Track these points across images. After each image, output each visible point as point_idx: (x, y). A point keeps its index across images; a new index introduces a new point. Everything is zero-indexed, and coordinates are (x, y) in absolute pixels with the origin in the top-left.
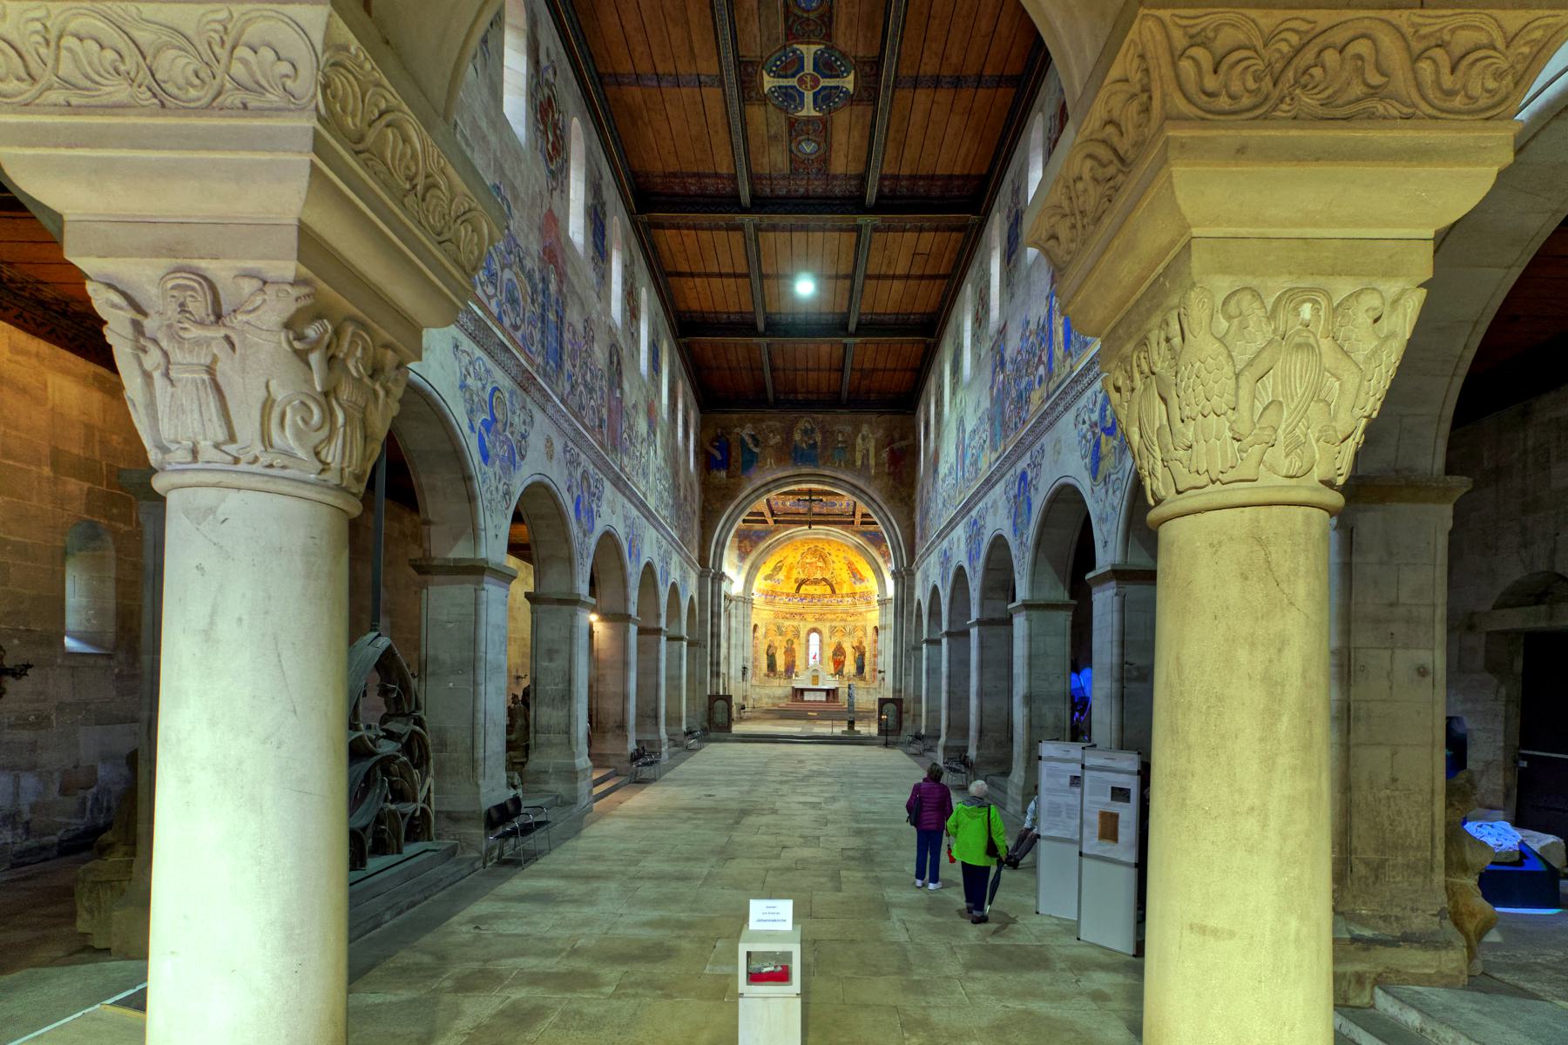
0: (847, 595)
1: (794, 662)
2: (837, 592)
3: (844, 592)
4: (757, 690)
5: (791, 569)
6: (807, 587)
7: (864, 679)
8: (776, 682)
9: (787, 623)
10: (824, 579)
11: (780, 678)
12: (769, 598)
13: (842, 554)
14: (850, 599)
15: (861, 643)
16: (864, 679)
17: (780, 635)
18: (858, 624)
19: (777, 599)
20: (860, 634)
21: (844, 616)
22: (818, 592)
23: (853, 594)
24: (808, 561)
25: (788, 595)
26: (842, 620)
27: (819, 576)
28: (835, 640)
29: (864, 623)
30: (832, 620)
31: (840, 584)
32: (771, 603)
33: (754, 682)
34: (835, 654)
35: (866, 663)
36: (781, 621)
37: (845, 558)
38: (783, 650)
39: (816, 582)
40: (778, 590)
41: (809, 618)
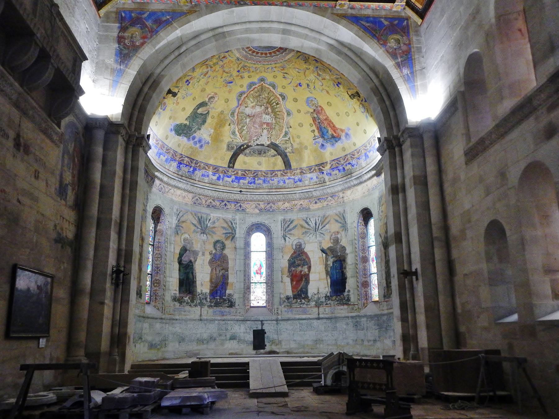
0: (310, 169)
1: (225, 278)
2: (294, 165)
3: (304, 165)
4: (158, 326)
5: (220, 124)
6: (248, 159)
7: (346, 302)
8: (195, 312)
9: (214, 215)
10: (274, 146)
11: (201, 305)
12: (185, 169)
13: (303, 94)
14: (314, 175)
15: (336, 241)
16: (346, 302)
17: (203, 232)
18: (330, 212)
19: (198, 173)
20: (334, 227)
21: (305, 203)
22: (264, 168)
23: (320, 167)
24: (248, 111)
25: (216, 169)
26: (302, 209)
27: (265, 140)
28: (292, 241)
29: (340, 209)
30: (285, 211)
31: (298, 152)
32: (189, 177)
33: (149, 310)
34: (292, 264)
35: (349, 272)
36: (205, 210)
37: (309, 101)
38: (208, 257)
39: (261, 151)
40: (200, 158)
41: (250, 208)
